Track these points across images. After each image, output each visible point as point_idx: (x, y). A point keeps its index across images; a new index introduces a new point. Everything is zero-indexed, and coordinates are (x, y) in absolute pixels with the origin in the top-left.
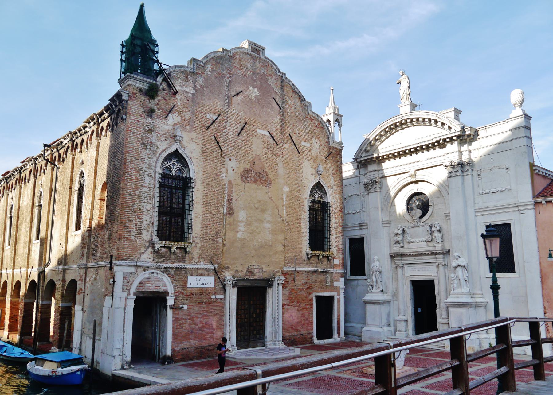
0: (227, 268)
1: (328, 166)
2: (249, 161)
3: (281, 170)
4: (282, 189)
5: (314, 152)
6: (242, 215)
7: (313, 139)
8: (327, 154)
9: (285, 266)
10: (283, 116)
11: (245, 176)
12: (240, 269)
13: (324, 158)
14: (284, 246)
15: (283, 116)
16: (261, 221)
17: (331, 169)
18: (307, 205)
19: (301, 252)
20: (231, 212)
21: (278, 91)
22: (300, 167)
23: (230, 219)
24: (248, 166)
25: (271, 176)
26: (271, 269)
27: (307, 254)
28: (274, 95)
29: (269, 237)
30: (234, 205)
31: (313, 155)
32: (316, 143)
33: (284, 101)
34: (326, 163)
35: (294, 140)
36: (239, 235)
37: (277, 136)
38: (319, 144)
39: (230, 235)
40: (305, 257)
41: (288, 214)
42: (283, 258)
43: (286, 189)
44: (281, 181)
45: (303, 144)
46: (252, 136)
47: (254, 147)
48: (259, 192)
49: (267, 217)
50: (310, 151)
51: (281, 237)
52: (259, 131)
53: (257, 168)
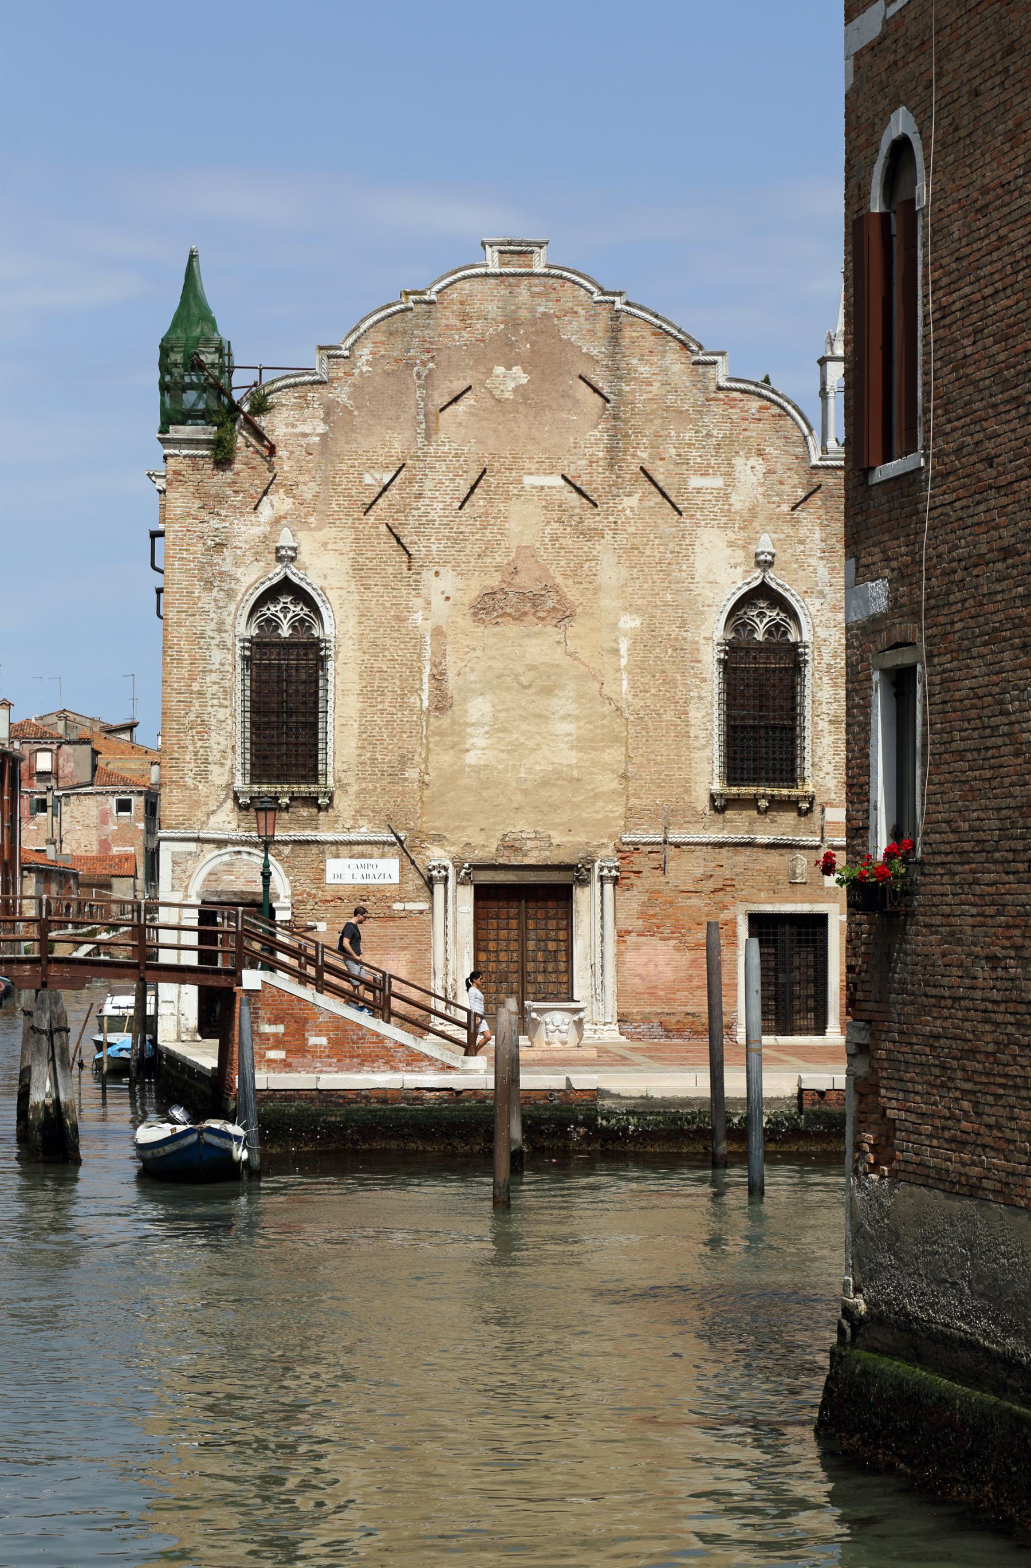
0: (439, 839)
1: (803, 532)
2: (498, 568)
3: (610, 571)
4: (614, 626)
5: (739, 501)
6: (478, 708)
7: (738, 461)
8: (801, 493)
9: (626, 829)
10: (616, 417)
11: (487, 607)
12: (478, 839)
13: (786, 508)
14: (624, 777)
15: (616, 417)
16: (543, 718)
17: (818, 535)
18: (710, 657)
19: (688, 791)
20: (442, 704)
21: (597, 349)
22: (682, 550)
23: (445, 721)
24: (494, 581)
25: (572, 594)
26: (582, 838)
27: (712, 798)
28: (582, 368)
29: (573, 757)
30: (452, 682)
31: (737, 506)
32: (749, 472)
33: (617, 374)
34: (796, 523)
35: (659, 478)
36: (471, 758)
37: (595, 480)
38: (761, 468)
39: (442, 759)
40: (703, 803)
41: (638, 691)
42: (620, 810)
43: (630, 622)
44: (608, 602)
45: (695, 482)
46: (508, 499)
47: (513, 527)
48: (539, 646)
49: (563, 703)
50: (727, 497)
51: (613, 755)
52: (528, 480)
53: (524, 580)
